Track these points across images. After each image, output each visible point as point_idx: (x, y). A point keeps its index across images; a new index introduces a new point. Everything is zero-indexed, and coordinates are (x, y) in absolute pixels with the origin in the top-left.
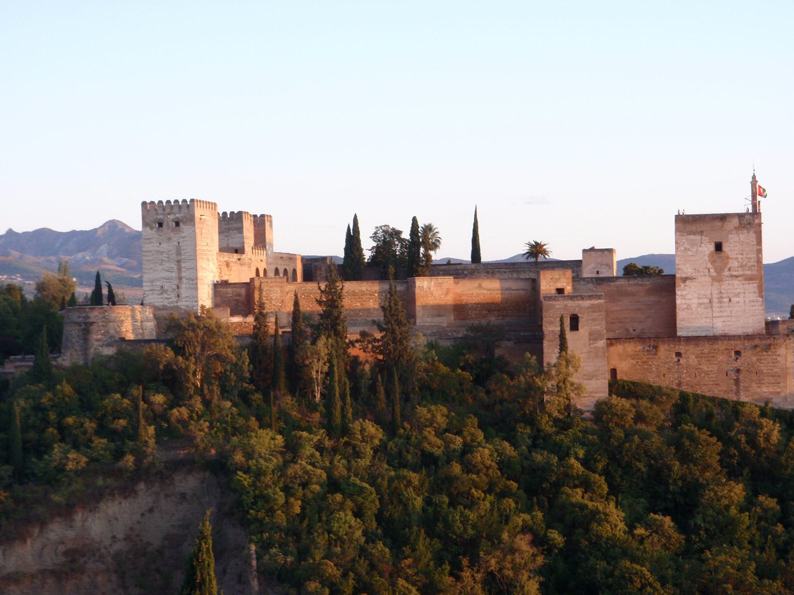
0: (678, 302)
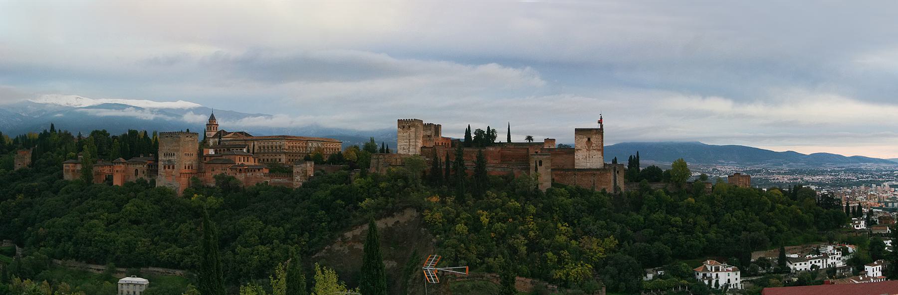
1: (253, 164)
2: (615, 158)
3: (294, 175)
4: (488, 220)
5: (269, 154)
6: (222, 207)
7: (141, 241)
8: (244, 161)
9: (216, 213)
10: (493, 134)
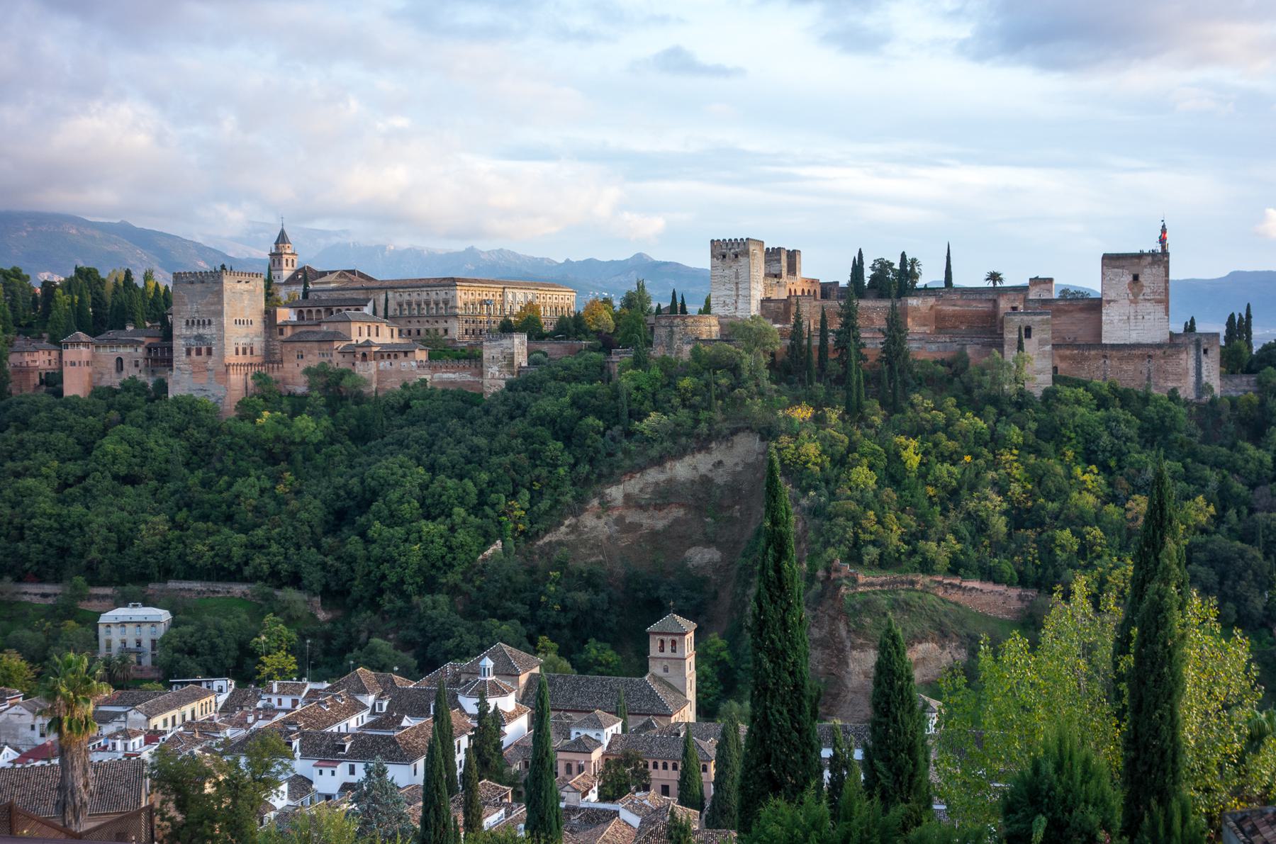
0: (1104, 318)
1: (388, 340)
2: (1192, 321)
3: (485, 363)
4: (918, 459)
5: (421, 319)
6: (328, 439)
7: (146, 523)
8: (369, 335)
9: (318, 451)
10: (913, 268)
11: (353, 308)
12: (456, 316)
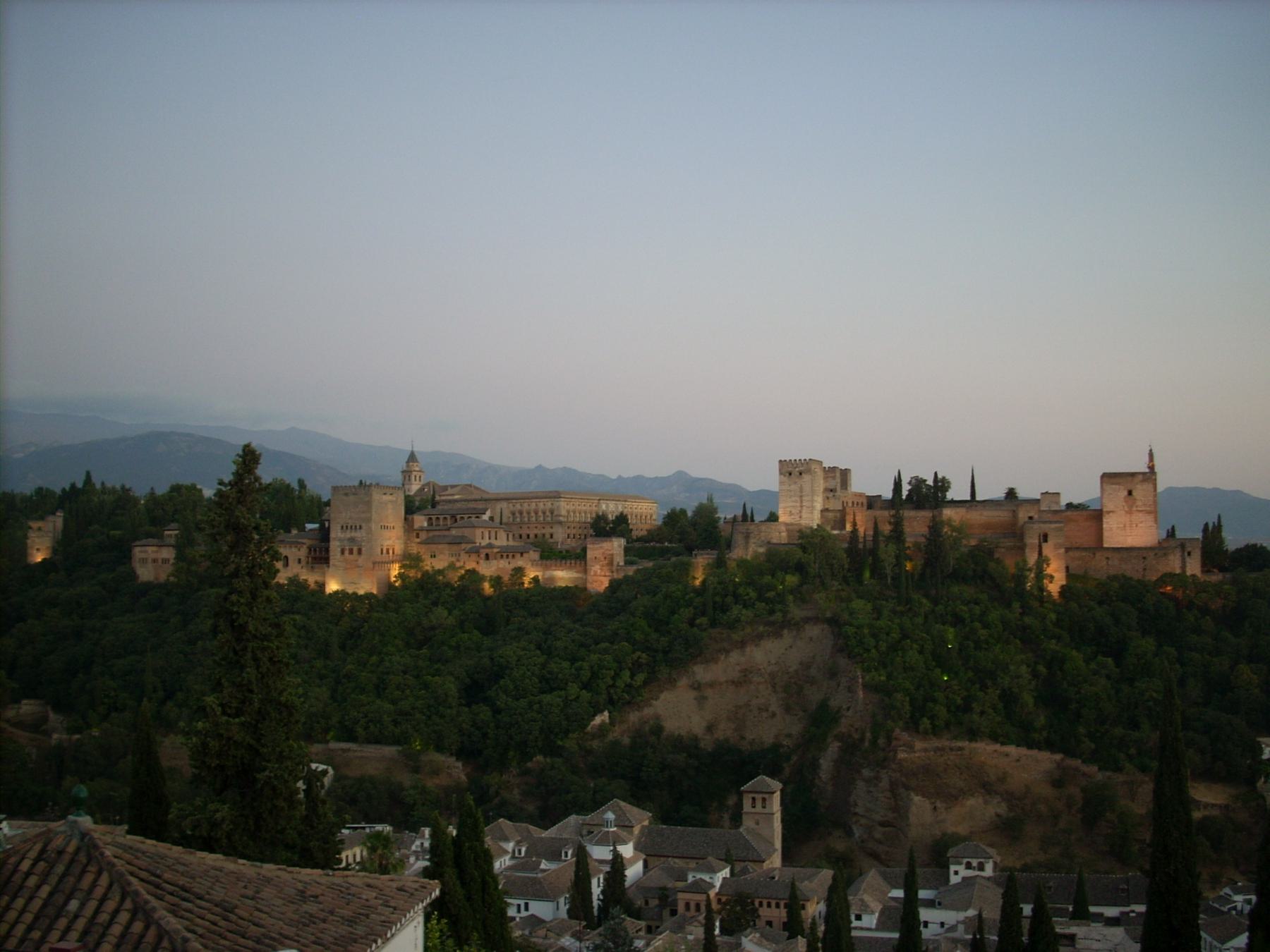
0: (1104, 526)
1: (505, 543)
2: (1173, 528)
3: (589, 562)
8: (490, 538)
10: (943, 484)
11: (474, 516)
12: (560, 523)
